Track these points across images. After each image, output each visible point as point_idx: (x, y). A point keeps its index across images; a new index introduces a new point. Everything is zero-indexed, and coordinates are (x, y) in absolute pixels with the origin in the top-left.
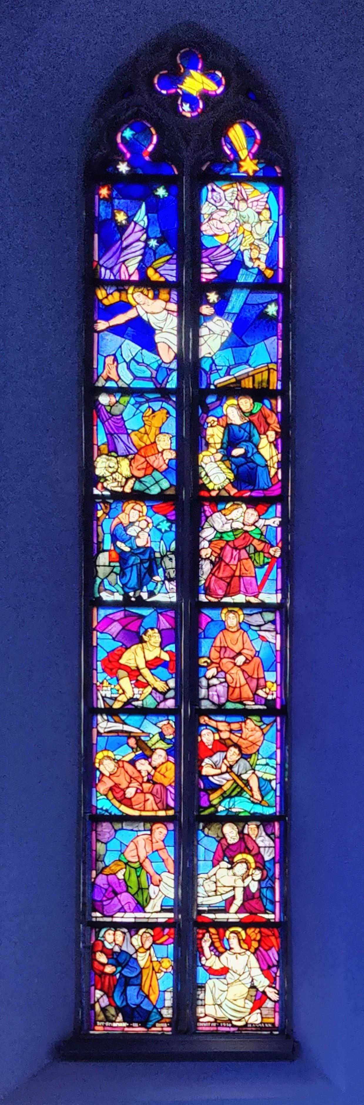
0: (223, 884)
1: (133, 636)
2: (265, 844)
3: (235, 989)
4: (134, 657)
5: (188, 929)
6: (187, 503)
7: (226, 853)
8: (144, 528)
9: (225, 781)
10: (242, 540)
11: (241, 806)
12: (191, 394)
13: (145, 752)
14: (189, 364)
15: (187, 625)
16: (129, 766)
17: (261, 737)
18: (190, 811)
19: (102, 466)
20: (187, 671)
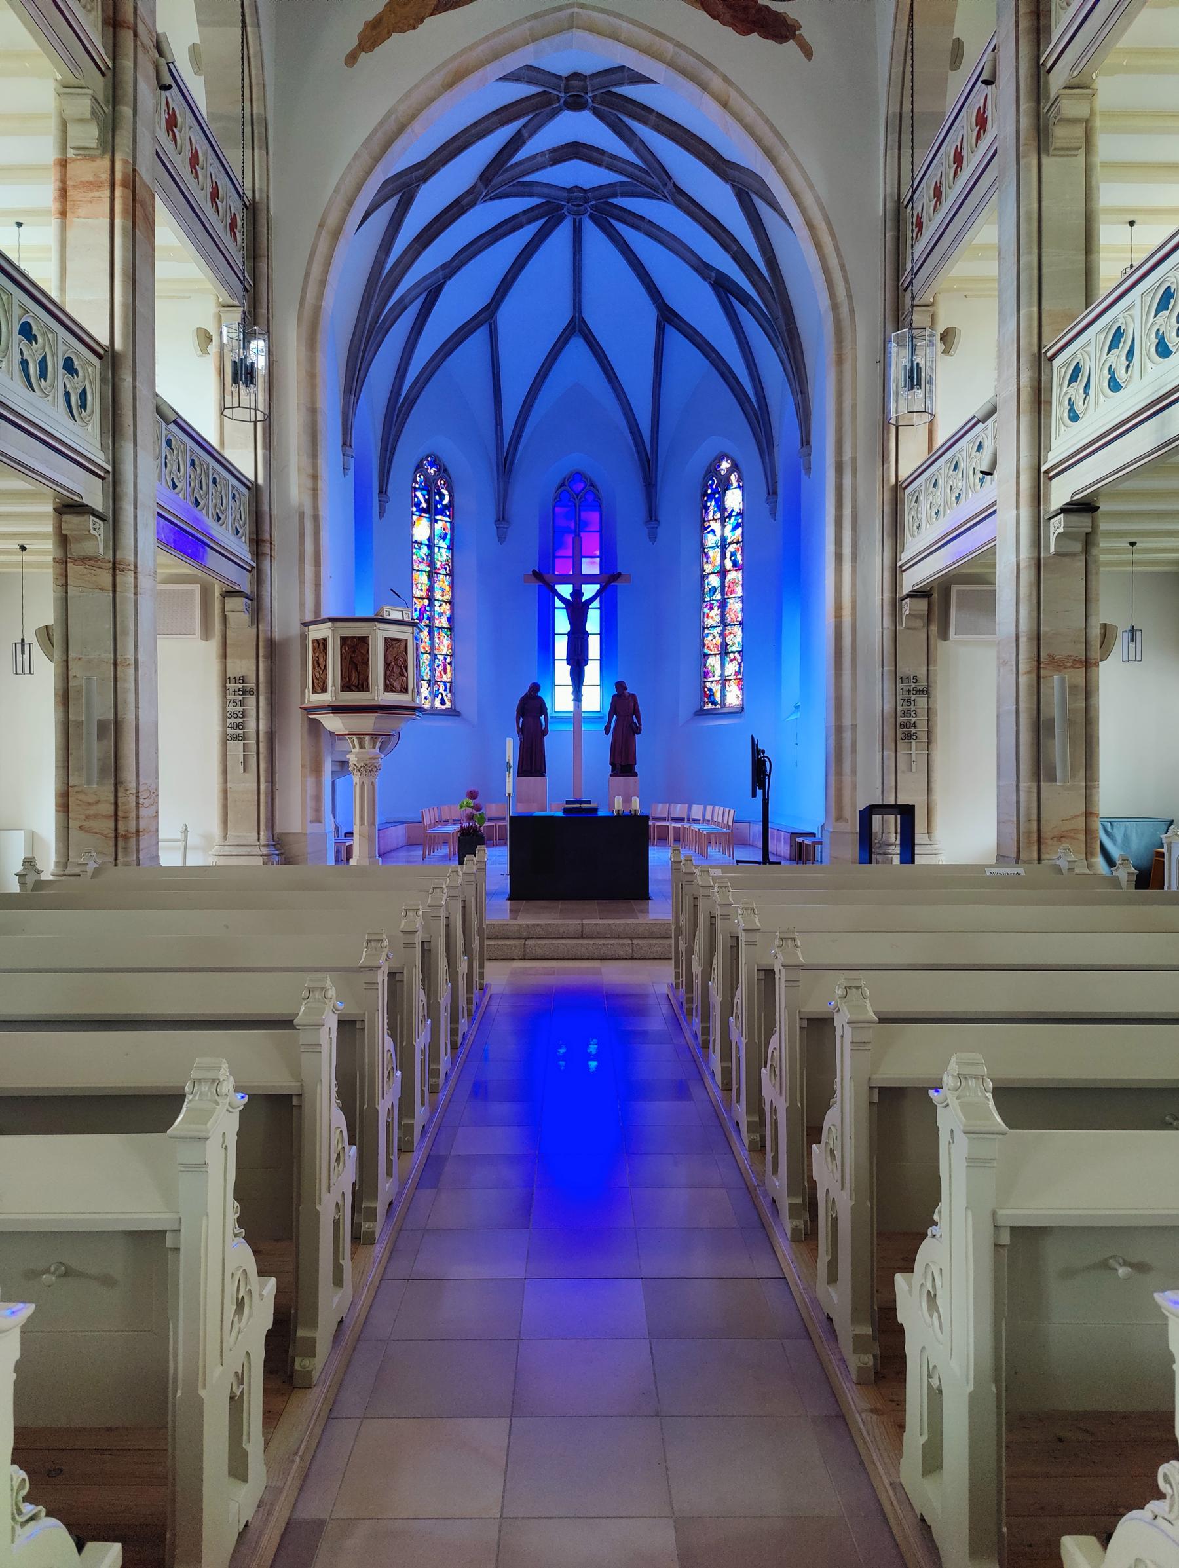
0: (731, 668)
1: (711, 609)
2: (739, 657)
3: (733, 696)
4: (712, 613)
5: (724, 681)
6: (723, 573)
7: (731, 661)
8: (714, 581)
9: (730, 643)
10: (734, 582)
11: (734, 649)
12: (724, 545)
13: (714, 637)
14: (723, 539)
15: (723, 604)
16: (712, 641)
17: (738, 631)
18: (724, 651)
19: (706, 567)
20: (723, 616)
